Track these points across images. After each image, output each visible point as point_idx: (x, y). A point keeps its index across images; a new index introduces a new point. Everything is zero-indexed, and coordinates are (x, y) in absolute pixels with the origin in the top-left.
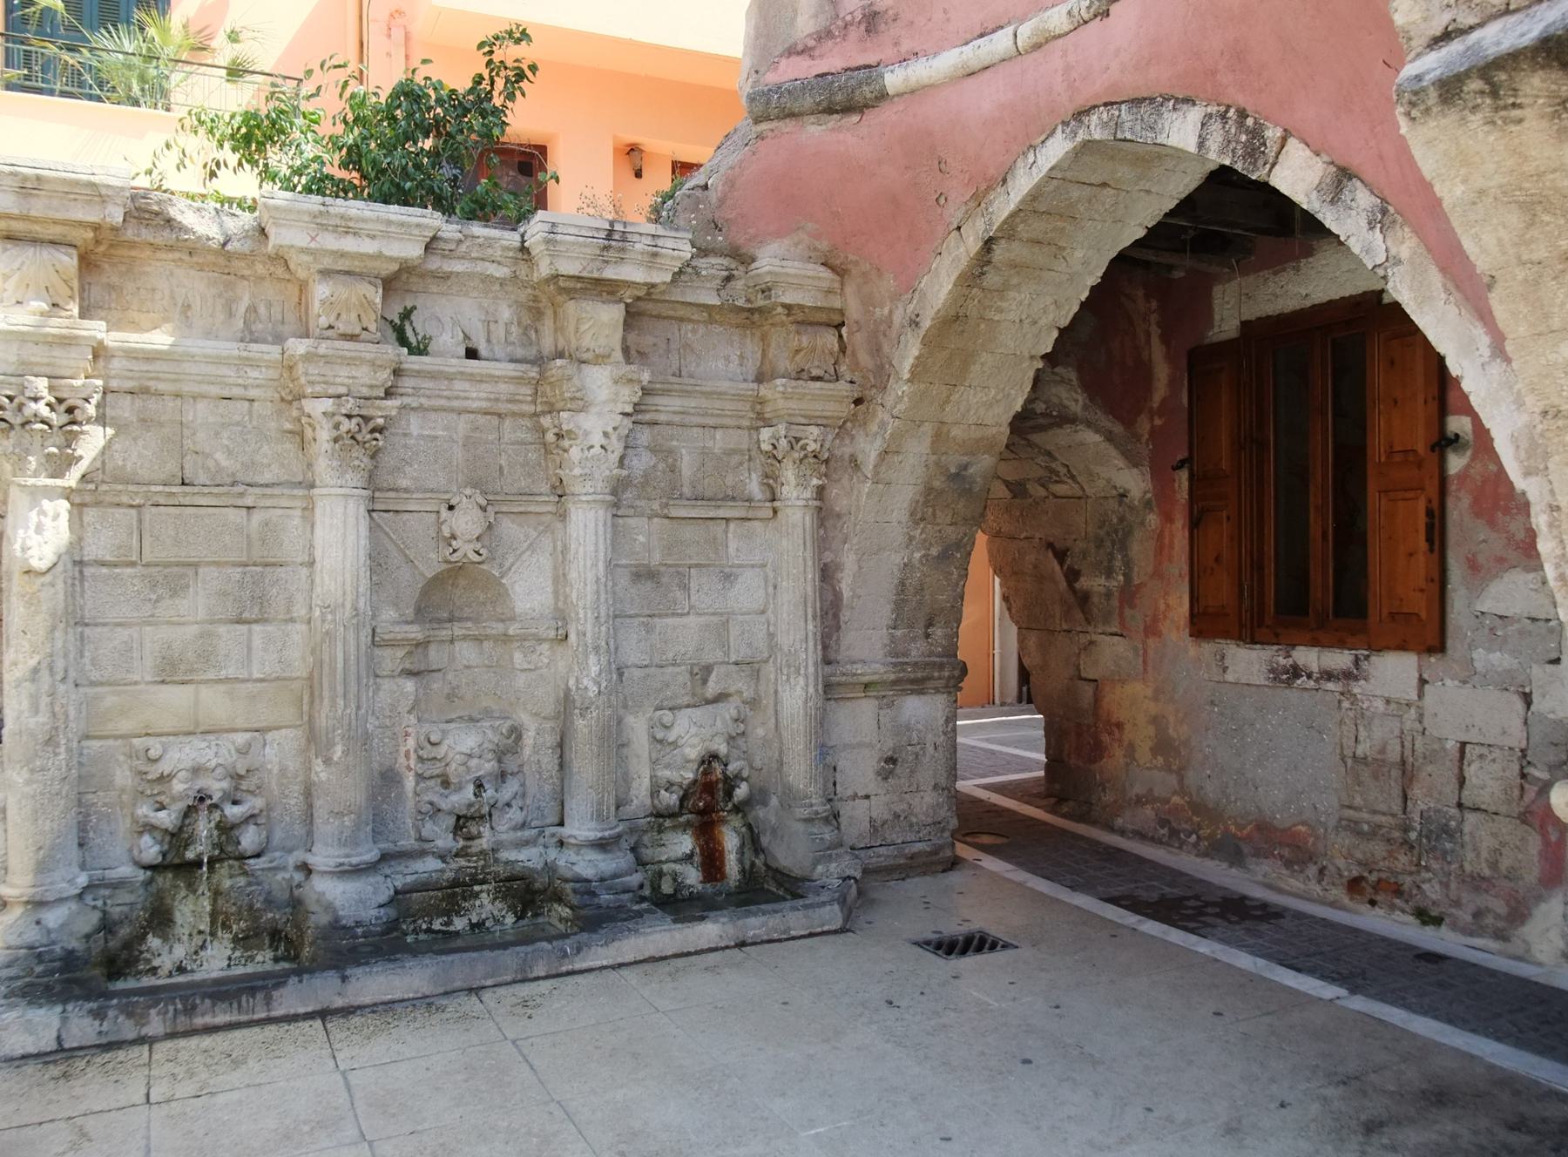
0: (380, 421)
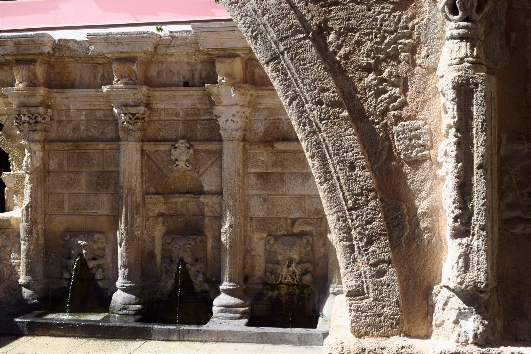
0: (137, 115)
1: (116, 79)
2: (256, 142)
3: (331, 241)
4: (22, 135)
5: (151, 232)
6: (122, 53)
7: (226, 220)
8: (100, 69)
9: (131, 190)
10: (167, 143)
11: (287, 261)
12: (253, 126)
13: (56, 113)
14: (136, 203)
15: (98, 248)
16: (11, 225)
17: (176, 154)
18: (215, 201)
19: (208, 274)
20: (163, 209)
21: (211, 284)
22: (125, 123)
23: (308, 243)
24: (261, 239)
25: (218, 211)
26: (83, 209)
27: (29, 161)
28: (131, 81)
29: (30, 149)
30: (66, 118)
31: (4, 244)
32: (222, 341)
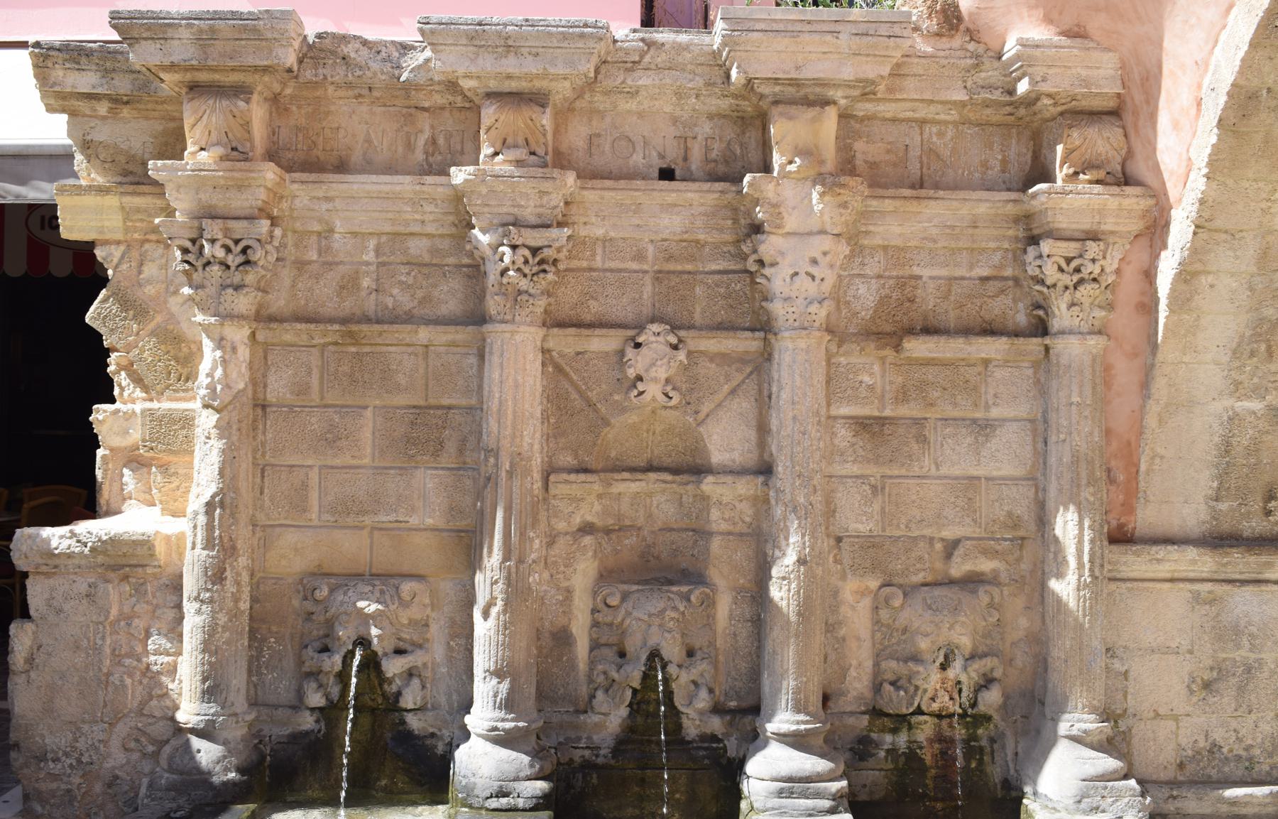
0: (547, 253)
1: (486, 150)
2: (854, 335)
3: (1065, 598)
4: (198, 299)
5: (561, 576)
6: (509, 77)
7: (788, 545)
8: (424, 122)
9: (521, 459)
10: (612, 332)
11: (942, 653)
12: (845, 292)
13: (290, 240)
14: (533, 496)
15: (413, 623)
16: (152, 555)
17: (638, 362)
18: (742, 492)
19: (717, 693)
20: (590, 512)
21: (728, 718)
22: (511, 273)
23: (991, 605)
24: (862, 593)
25: (748, 519)
26: (364, 513)
27: (219, 373)
28: (533, 157)
29: (222, 339)
30: (320, 255)
31: (126, 609)
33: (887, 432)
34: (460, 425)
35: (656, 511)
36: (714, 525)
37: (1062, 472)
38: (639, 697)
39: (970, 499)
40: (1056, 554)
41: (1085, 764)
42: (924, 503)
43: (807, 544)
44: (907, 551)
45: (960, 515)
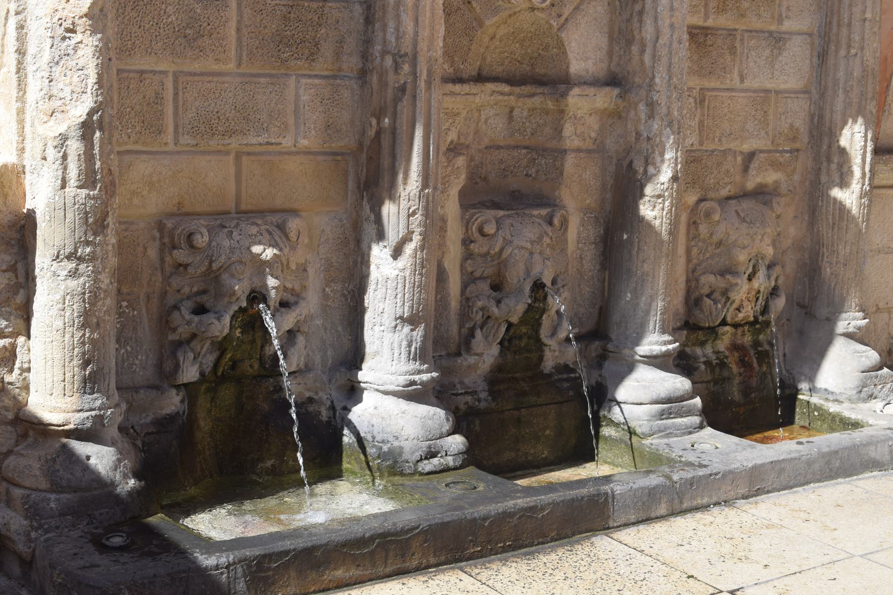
7: (663, 161)
26: (230, 133)
32: (758, 492)
33: (709, 43)
34: (338, 22)
35: (484, 126)
36: (568, 141)
37: (852, 86)
38: (512, 331)
39: (765, 112)
40: (840, 166)
41: (862, 356)
42: (733, 116)
43: (679, 160)
44: (719, 164)
45: (757, 127)
